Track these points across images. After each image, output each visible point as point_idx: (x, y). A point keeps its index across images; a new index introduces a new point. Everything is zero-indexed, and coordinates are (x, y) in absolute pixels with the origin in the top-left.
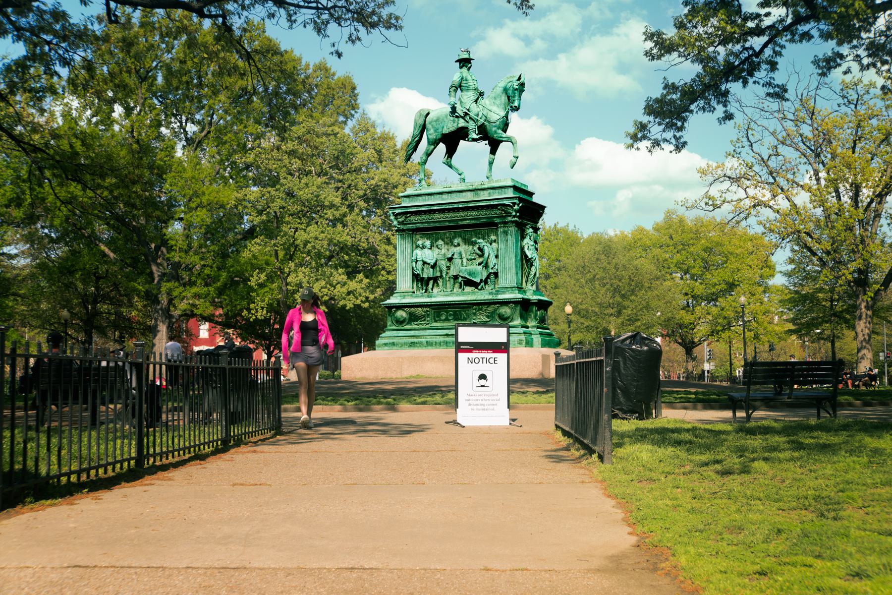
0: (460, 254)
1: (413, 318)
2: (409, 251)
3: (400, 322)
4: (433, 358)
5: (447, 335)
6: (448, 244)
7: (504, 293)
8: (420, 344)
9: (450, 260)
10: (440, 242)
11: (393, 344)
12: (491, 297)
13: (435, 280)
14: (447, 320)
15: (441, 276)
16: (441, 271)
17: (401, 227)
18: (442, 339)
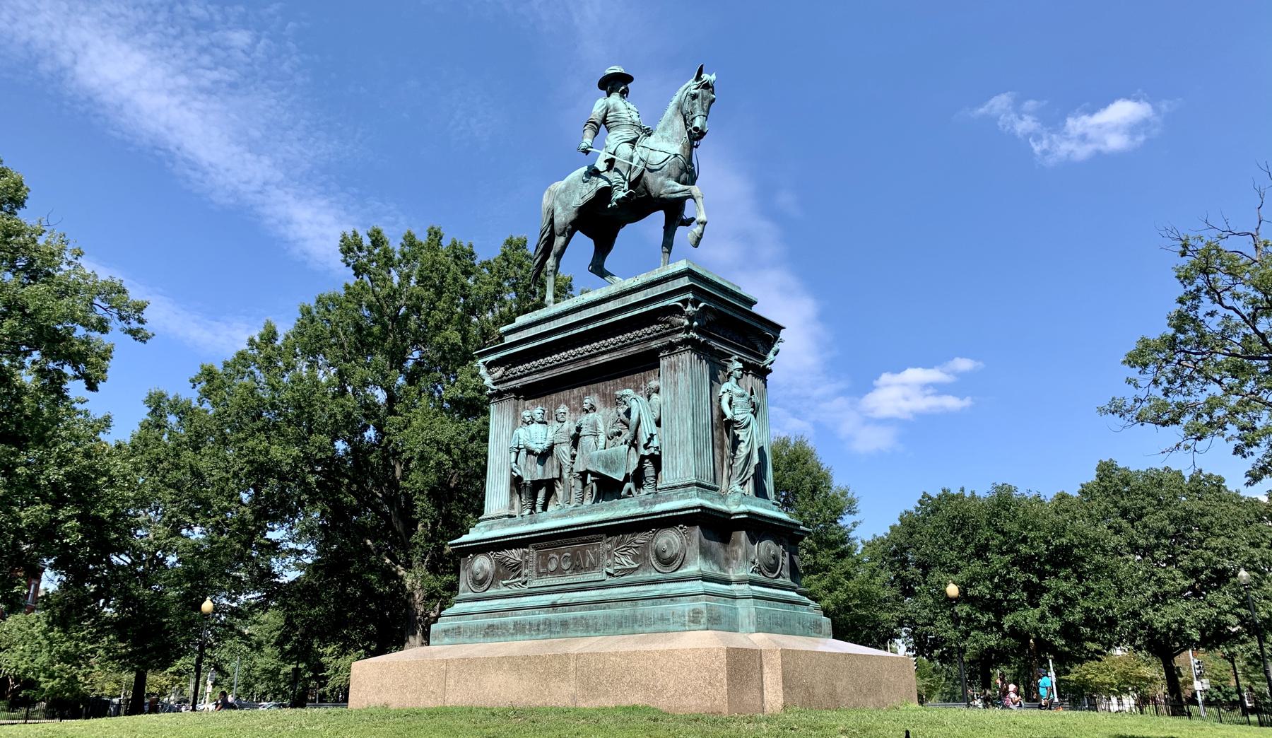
0: (595, 425)
1: (508, 571)
2: (508, 431)
5: (554, 606)
6: (575, 410)
7: (668, 499)
8: (504, 626)
10: (563, 409)
12: (640, 510)
14: (559, 571)
15: (560, 478)
18: (541, 616)
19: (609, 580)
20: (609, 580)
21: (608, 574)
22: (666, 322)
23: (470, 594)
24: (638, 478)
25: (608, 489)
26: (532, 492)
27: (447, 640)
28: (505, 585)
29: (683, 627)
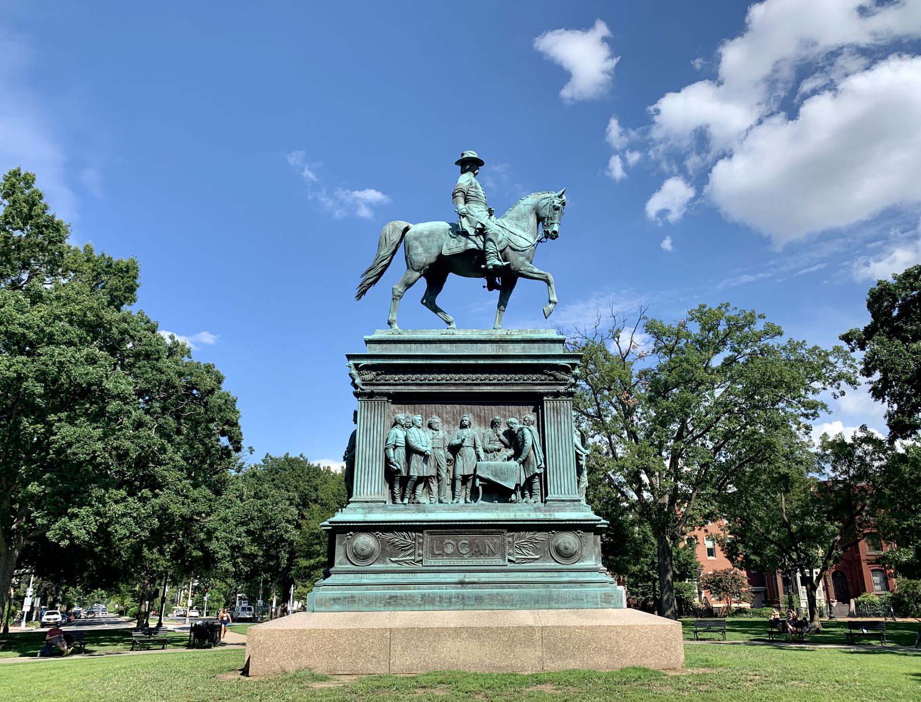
3: (363, 557)
4: (457, 632)
5: (462, 583)
6: (448, 422)
7: (560, 510)
9: (455, 449)
11: (352, 599)
13: (424, 480)
14: (457, 554)
15: (438, 475)
16: (438, 467)
17: (368, 389)
18: (452, 591)
19: (511, 566)
20: (511, 566)
21: (510, 561)
22: (551, 375)
23: (349, 567)
24: (526, 488)
25: (496, 492)
26: (399, 482)
27: (337, 607)
28: (395, 562)
29: (596, 606)
